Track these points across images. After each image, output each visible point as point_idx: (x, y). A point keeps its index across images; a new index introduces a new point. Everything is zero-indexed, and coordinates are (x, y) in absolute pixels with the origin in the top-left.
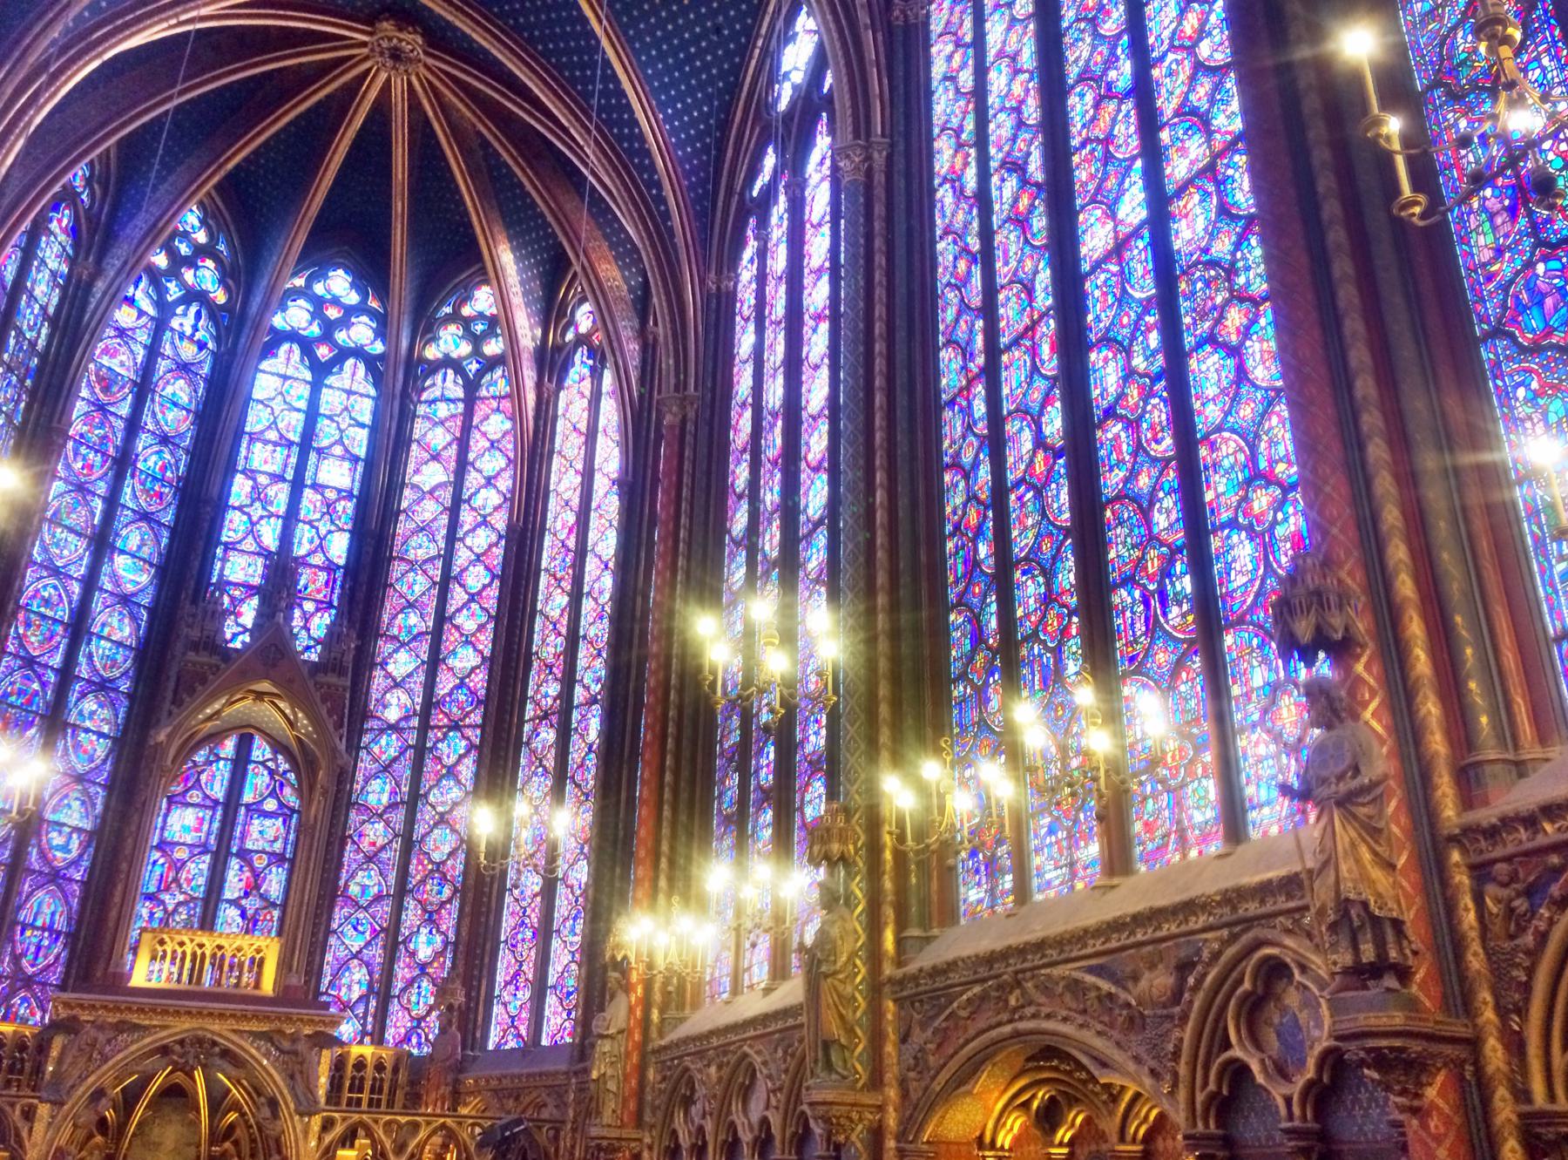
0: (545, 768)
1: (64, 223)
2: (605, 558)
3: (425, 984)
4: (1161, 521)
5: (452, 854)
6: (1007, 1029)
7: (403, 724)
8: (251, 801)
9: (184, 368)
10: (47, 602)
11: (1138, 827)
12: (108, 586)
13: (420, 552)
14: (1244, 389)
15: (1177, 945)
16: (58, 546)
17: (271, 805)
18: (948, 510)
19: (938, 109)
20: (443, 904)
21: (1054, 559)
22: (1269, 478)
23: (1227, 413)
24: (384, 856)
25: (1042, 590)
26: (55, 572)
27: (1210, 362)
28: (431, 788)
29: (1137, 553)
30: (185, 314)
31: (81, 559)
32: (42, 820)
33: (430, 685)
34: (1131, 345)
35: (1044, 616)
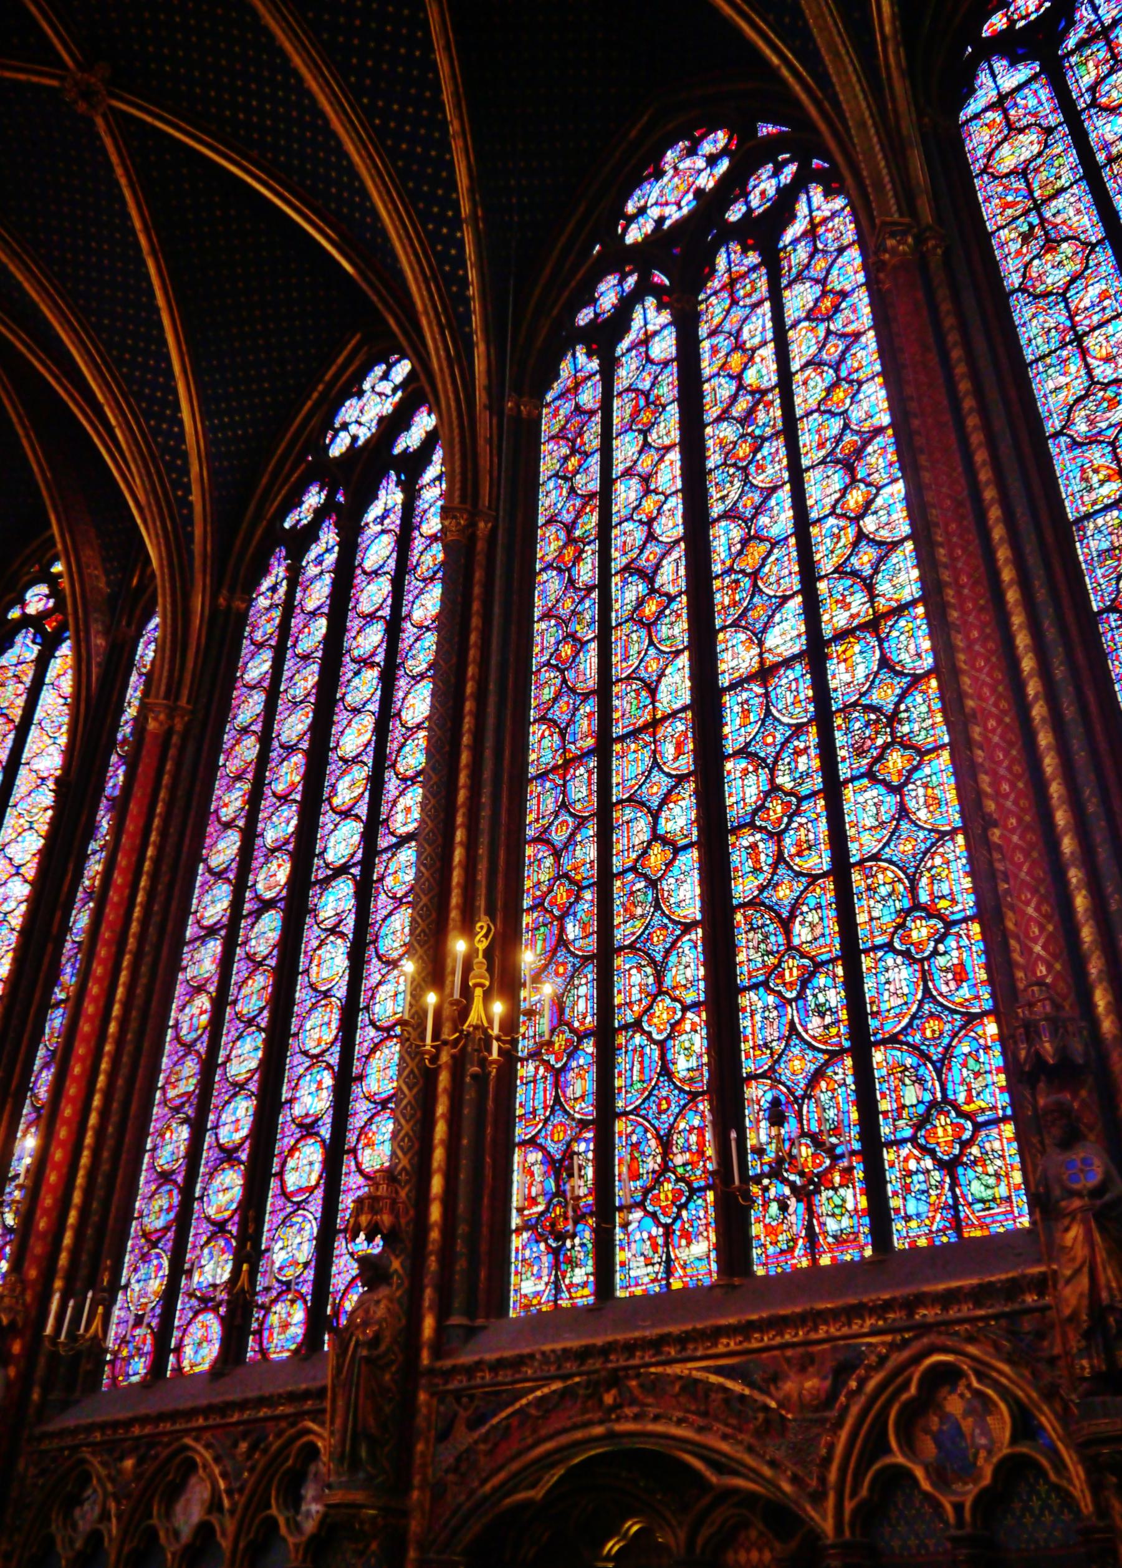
2: (17, 862)
4: (801, 934)
6: (599, 1430)
11: (756, 1229)
14: (905, 825)
15: (835, 1349)
18: (528, 884)
19: (544, 502)
21: (667, 953)
22: (931, 912)
23: (887, 844)
25: (651, 980)
27: (868, 795)
29: (771, 960)
34: (775, 763)
35: (650, 1007)
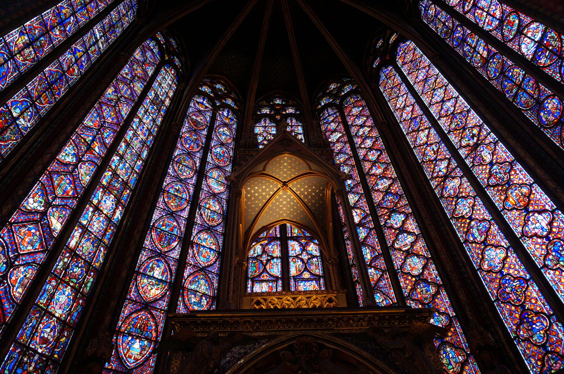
0: (463, 197)
1: (173, 72)
3: (448, 349)
5: (425, 267)
7: (364, 221)
8: (296, 275)
9: (225, 125)
10: (177, 191)
12: (205, 189)
13: (341, 160)
16: (181, 171)
17: (306, 275)
20: (434, 296)
24: (381, 284)
26: (181, 181)
28: (394, 242)
30: (224, 111)
31: (192, 177)
32: (184, 288)
33: (370, 201)
